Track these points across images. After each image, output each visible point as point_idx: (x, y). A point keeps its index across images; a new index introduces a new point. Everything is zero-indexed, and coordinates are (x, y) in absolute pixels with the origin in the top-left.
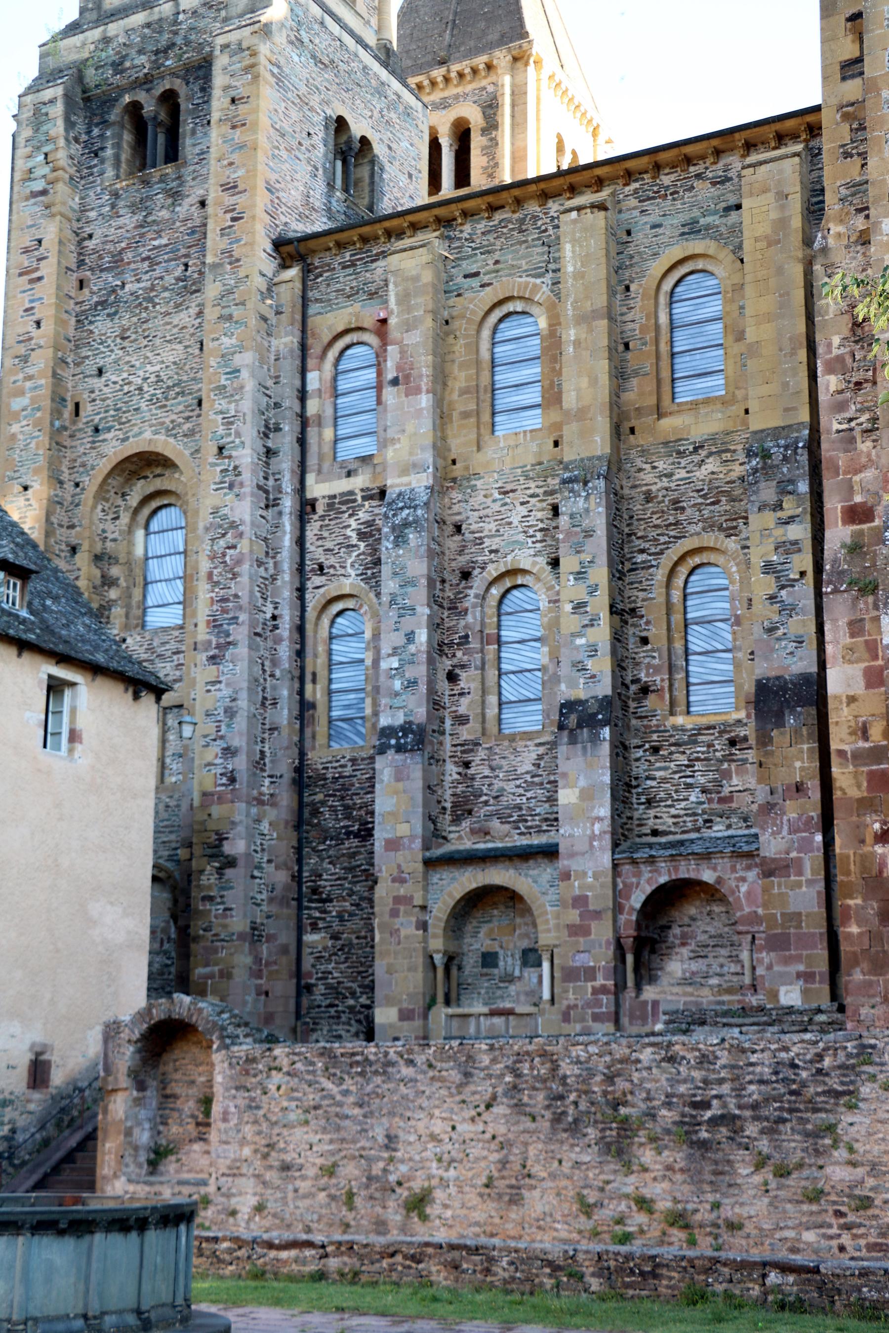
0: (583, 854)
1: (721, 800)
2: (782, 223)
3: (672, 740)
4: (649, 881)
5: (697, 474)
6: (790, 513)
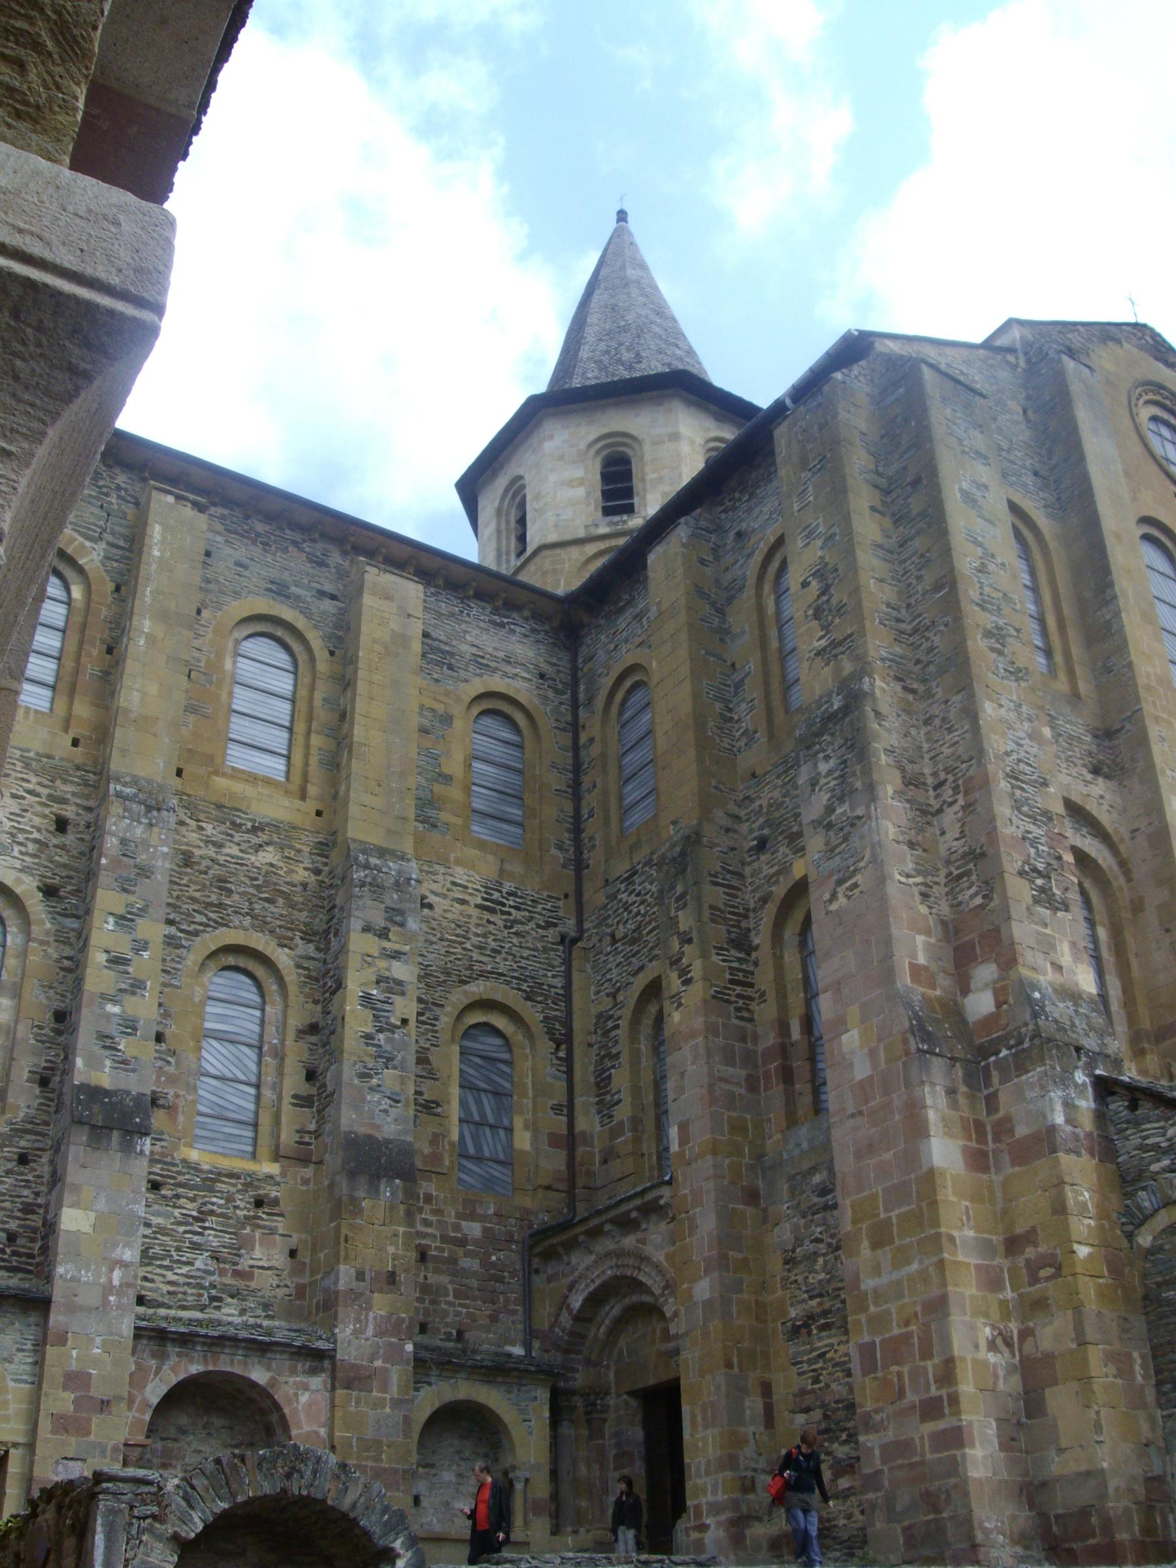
0: (90, 1310)
1: (236, 1273)
2: (401, 639)
3: (181, 1178)
4: (174, 1369)
5: (253, 858)
6: (397, 947)
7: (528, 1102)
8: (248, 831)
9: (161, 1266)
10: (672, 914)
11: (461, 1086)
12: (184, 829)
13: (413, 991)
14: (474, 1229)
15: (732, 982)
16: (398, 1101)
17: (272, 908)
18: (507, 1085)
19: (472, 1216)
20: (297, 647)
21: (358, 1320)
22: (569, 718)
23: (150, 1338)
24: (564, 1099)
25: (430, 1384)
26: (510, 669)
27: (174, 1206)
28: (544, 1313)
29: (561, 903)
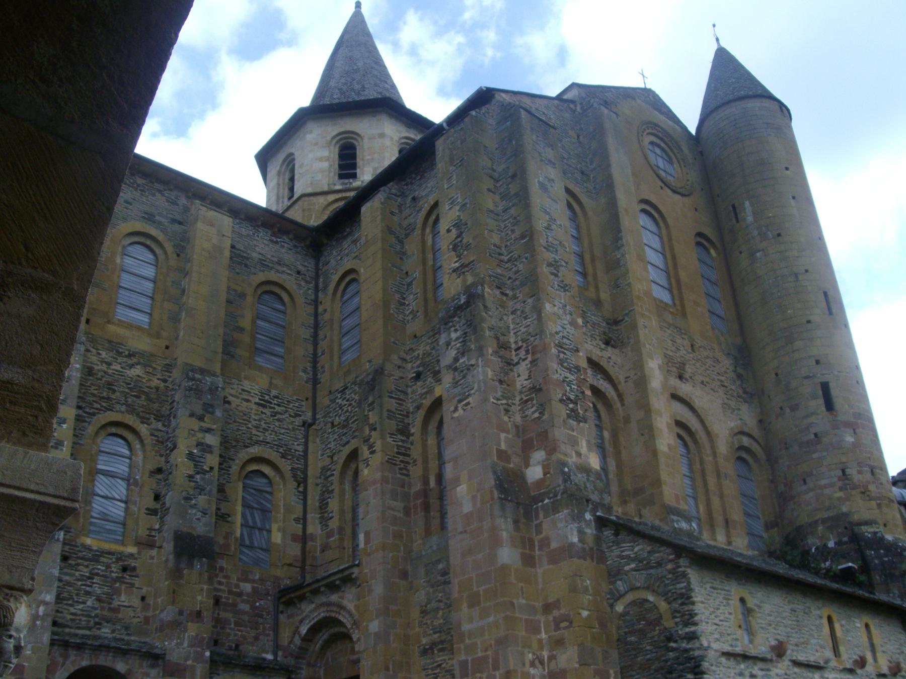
1: (111, 610)
3: (80, 554)
5: (128, 372)
6: (209, 426)
7: (281, 516)
8: (126, 356)
9: (67, 604)
10: (366, 413)
11: (243, 506)
12: (89, 354)
13: (217, 451)
14: (247, 587)
15: (398, 453)
16: (206, 514)
17: (138, 401)
18: (269, 506)
19: (246, 580)
20: (158, 251)
21: (179, 638)
22: (313, 297)
23: (59, 645)
24: (301, 514)
25: (218, 675)
26: (279, 268)
27: (76, 570)
28: (285, 636)
29: (304, 403)
